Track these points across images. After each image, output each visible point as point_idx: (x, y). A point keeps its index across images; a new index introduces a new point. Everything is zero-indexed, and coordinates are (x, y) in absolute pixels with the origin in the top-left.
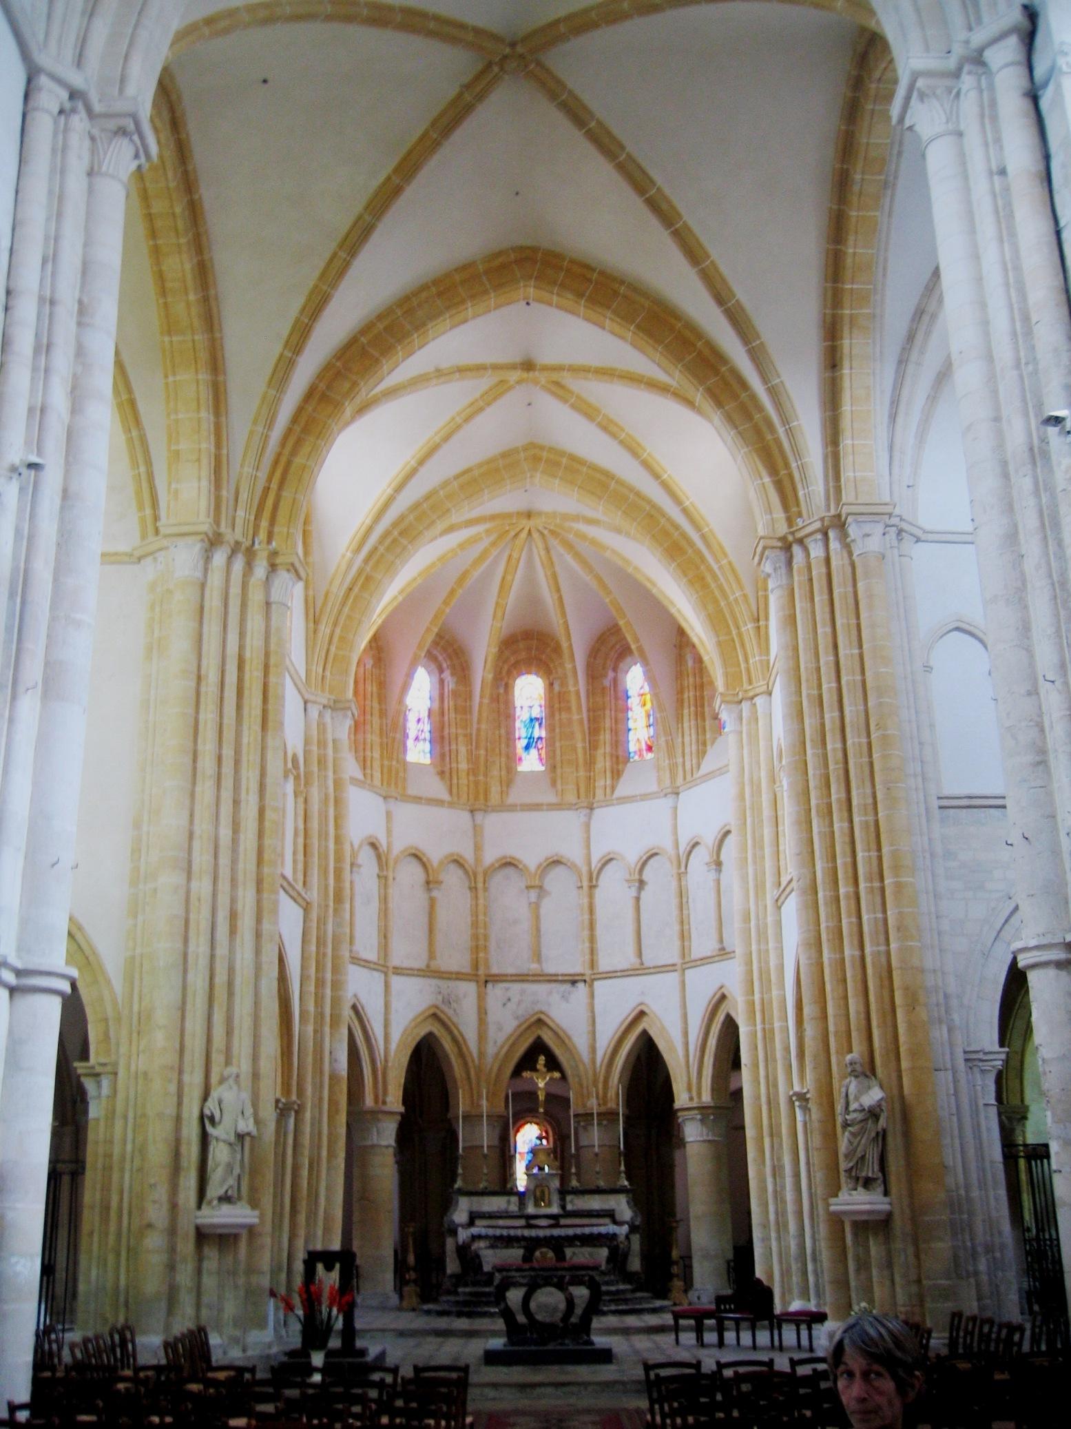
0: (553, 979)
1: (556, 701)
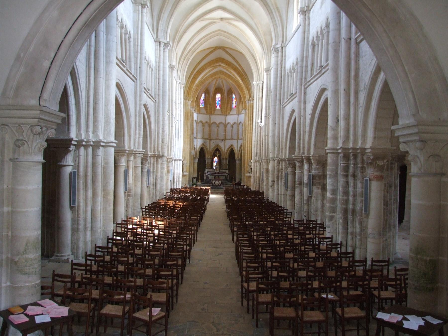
0: (220, 140)
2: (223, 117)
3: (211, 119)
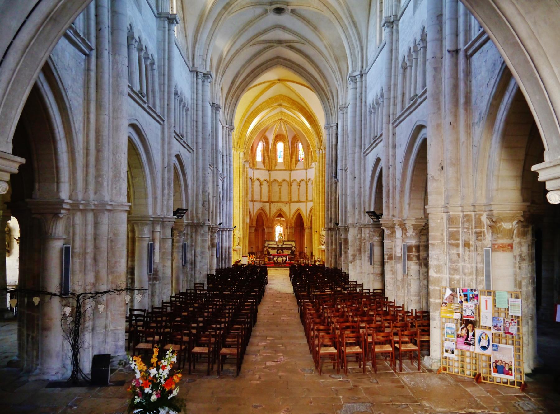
1: (285, 149)
2: (287, 173)
3: (272, 175)
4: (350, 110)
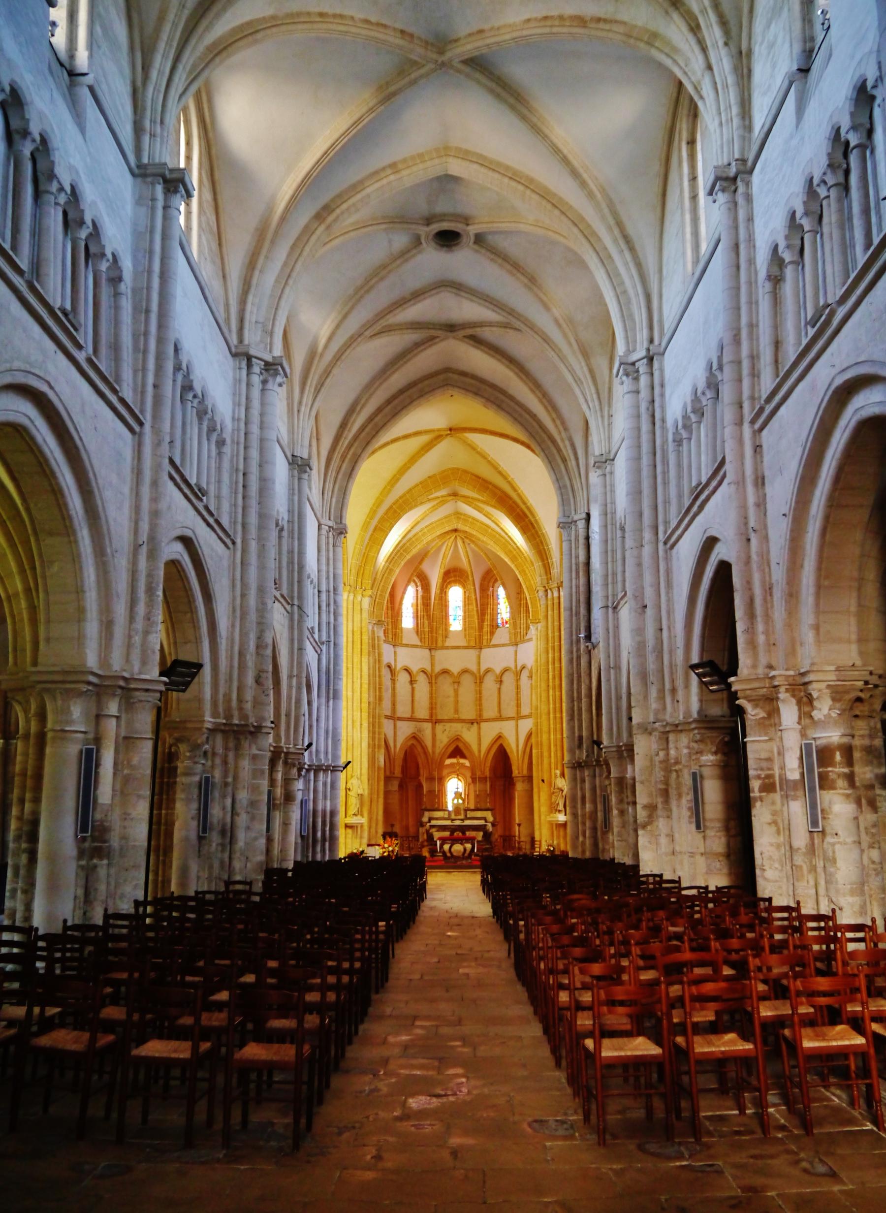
4: (621, 467)
